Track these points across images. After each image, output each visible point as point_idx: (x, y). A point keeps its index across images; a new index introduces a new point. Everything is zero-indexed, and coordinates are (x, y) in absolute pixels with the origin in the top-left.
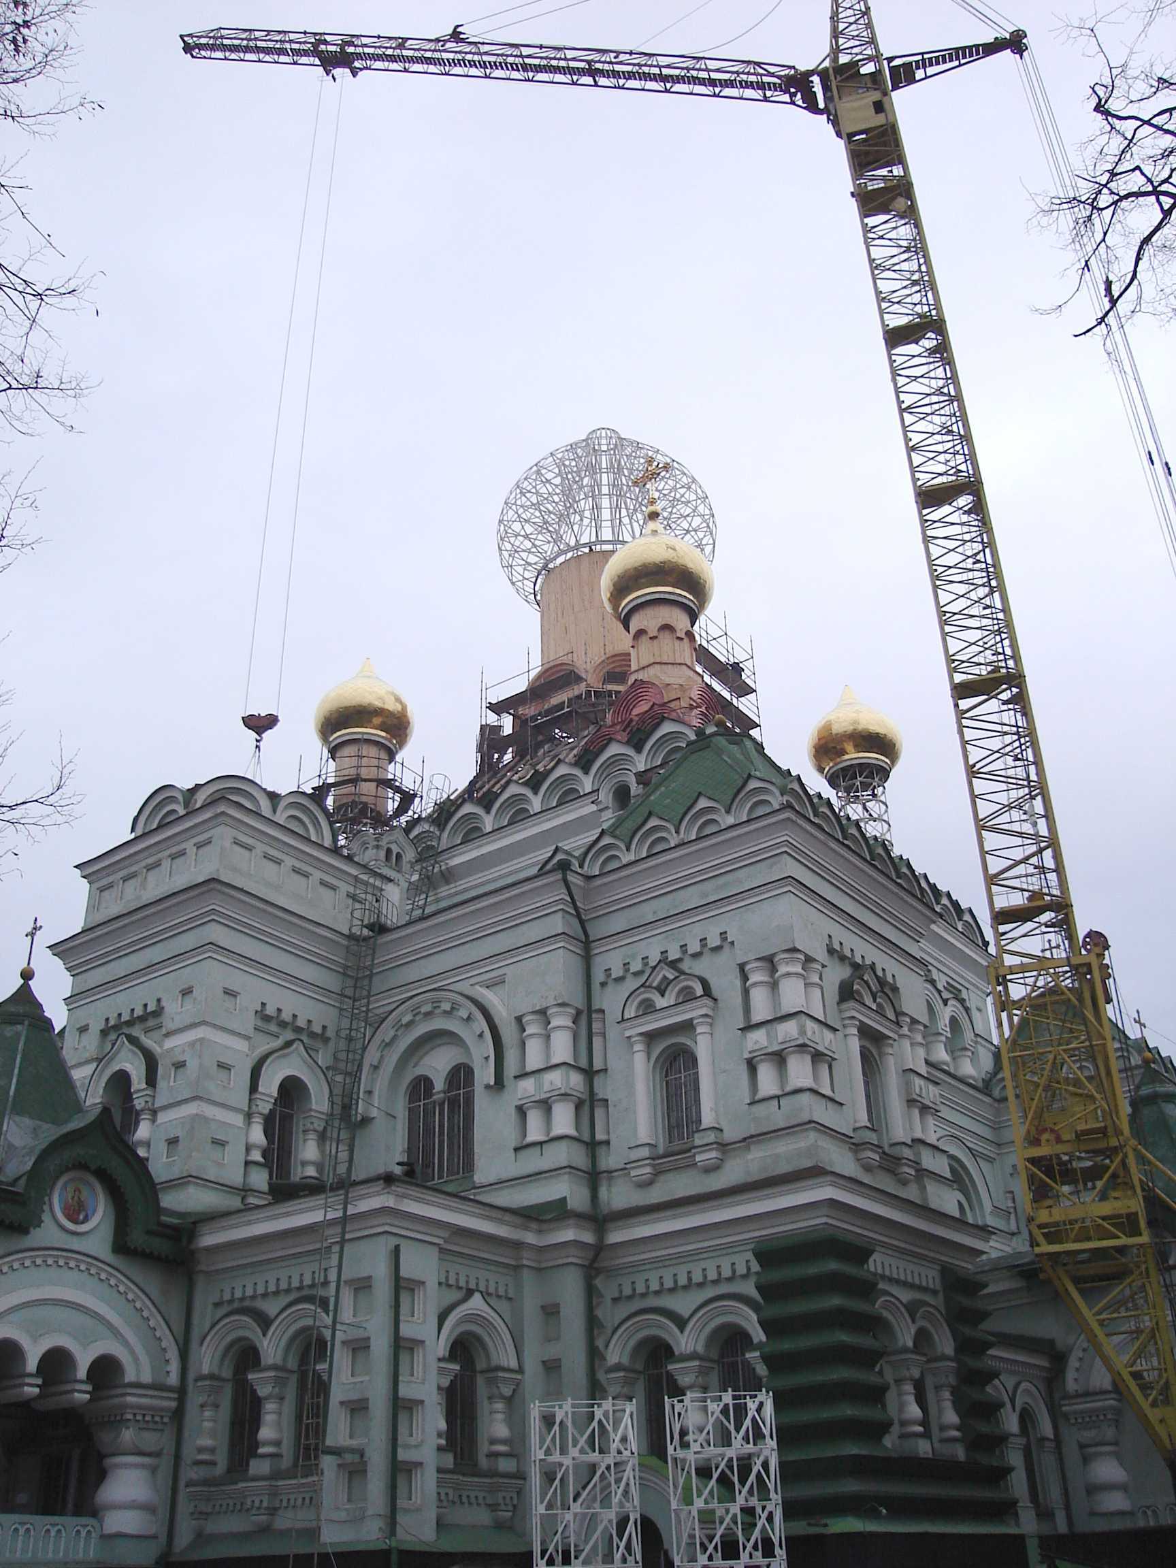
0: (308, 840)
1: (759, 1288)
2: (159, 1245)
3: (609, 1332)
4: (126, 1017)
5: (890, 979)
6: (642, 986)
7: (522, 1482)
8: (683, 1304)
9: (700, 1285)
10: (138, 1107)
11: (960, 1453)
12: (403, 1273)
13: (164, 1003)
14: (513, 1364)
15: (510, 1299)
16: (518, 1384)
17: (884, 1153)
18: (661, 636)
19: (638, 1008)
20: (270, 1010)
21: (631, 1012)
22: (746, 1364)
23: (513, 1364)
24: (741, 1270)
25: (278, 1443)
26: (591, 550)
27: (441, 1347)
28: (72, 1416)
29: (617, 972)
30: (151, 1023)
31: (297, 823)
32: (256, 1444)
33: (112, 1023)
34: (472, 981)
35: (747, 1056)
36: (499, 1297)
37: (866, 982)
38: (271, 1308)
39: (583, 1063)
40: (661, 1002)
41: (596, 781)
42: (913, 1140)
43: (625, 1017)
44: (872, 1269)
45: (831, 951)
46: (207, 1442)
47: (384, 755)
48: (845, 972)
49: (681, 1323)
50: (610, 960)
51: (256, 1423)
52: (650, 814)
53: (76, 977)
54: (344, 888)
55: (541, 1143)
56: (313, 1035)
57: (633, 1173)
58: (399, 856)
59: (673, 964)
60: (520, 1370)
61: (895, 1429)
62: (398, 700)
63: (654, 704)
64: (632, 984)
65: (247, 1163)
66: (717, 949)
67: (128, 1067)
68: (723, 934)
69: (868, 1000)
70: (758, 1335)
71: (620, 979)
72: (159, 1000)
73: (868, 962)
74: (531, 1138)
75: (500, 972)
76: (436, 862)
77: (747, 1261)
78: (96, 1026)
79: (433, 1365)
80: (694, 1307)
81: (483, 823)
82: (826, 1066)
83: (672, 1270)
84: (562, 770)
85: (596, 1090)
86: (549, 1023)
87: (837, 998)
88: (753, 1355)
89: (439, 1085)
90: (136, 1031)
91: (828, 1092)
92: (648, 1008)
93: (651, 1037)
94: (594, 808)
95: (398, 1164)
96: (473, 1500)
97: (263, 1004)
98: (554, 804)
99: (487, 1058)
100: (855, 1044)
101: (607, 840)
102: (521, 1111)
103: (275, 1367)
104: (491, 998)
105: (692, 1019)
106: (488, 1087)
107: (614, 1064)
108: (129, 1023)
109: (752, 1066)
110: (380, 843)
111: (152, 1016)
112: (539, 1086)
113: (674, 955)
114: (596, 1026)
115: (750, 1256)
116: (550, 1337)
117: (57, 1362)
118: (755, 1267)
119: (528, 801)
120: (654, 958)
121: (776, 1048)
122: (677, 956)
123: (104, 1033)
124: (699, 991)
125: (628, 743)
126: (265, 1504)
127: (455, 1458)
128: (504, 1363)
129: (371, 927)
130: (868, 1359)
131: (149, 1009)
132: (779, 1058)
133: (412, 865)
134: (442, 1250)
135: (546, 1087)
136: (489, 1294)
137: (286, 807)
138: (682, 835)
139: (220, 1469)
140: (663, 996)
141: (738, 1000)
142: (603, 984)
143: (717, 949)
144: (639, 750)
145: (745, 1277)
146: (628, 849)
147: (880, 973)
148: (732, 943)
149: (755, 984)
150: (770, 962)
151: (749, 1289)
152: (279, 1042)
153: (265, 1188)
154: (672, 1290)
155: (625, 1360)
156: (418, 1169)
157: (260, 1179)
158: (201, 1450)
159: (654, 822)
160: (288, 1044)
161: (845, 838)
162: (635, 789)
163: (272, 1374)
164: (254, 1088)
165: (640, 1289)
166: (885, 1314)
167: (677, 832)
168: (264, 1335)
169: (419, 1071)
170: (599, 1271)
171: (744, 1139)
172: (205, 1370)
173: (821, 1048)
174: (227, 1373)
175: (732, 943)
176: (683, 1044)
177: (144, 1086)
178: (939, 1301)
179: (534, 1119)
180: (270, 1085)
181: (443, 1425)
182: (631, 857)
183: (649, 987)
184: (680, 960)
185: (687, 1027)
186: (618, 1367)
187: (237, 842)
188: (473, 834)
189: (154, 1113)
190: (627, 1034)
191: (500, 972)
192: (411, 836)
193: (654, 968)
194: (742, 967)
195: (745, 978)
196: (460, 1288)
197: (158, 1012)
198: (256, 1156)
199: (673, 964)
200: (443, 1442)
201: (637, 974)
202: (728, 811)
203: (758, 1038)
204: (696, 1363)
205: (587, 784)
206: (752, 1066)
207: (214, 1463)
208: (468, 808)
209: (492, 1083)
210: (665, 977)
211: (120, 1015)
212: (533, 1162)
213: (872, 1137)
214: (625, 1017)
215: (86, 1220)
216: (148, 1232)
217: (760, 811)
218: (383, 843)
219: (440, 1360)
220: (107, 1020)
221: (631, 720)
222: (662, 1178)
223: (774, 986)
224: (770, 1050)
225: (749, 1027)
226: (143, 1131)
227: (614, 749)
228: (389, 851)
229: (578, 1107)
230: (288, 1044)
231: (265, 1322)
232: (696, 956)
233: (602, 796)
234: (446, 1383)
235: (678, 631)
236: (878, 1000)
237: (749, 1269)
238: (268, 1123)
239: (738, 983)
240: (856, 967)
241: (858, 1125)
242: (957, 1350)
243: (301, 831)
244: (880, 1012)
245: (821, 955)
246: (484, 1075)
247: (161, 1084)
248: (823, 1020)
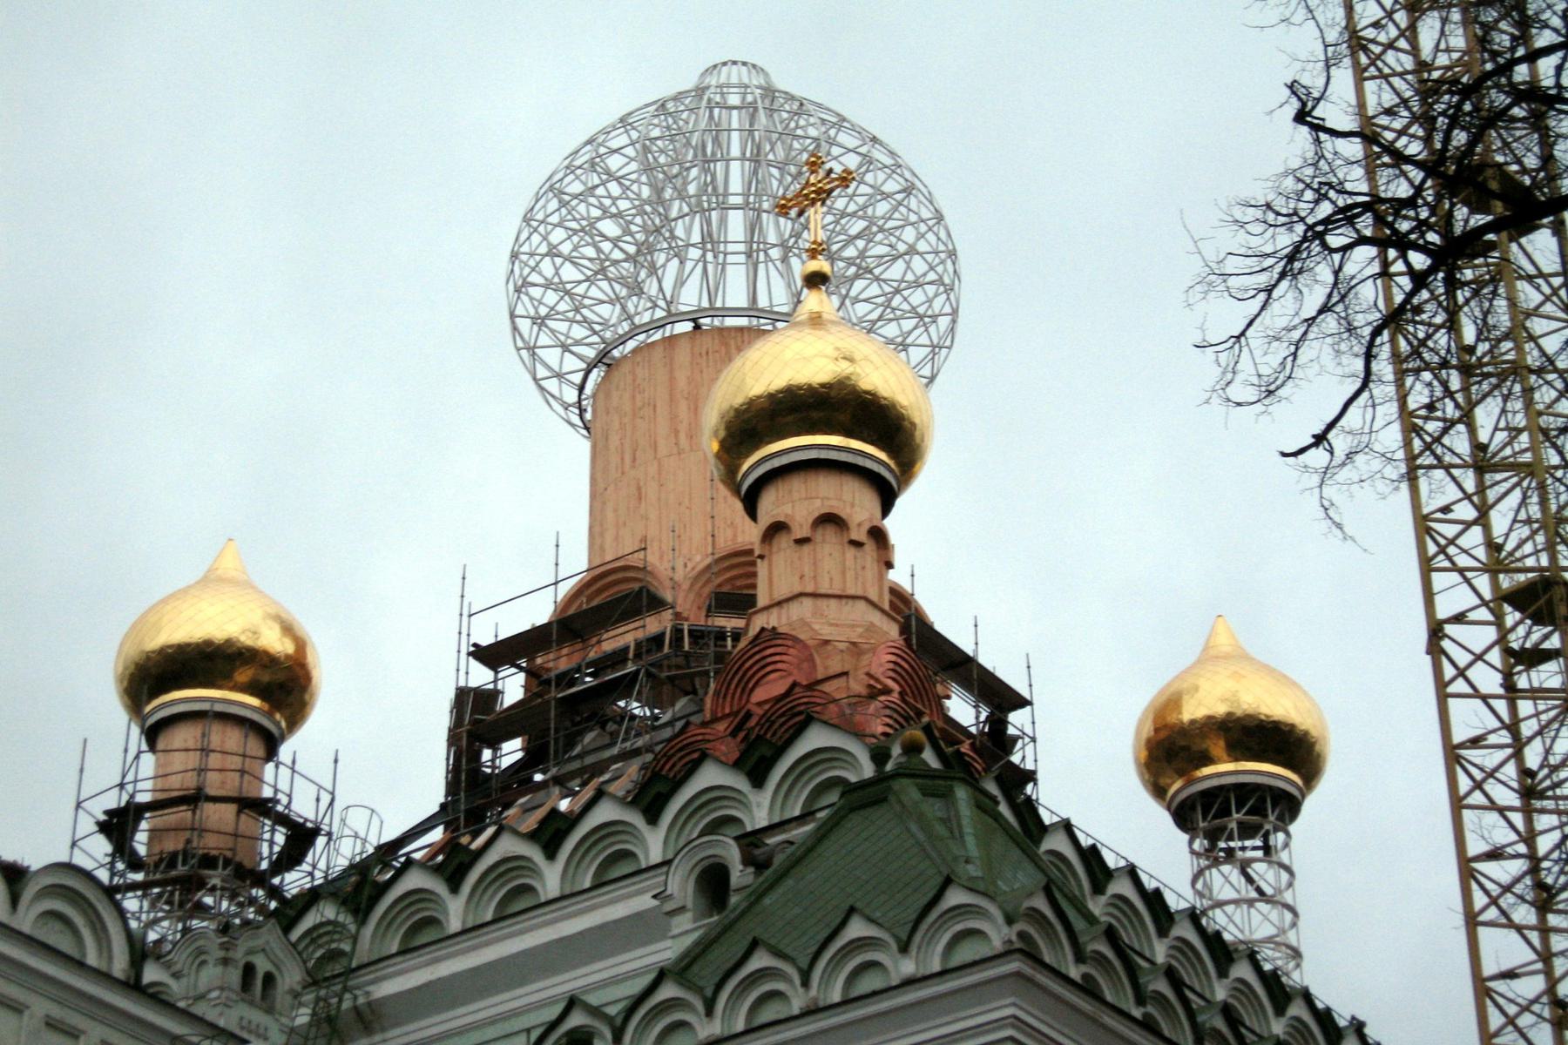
0: (79, 965)
18: (818, 536)
26: (697, 327)
31: (58, 926)
41: (673, 835)
47: (255, 747)
52: (754, 945)
58: (269, 979)
62: (288, 629)
63: (794, 685)
76: (345, 989)
81: (446, 912)
84: (605, 812)
98: (587, 884)
101: (668, 991)
110: (231, 954)
119: (534, 871)
125: (737, 765)
133: (296, 995)
138: (813, 992)
144: (758, 779)
146: (709, 1012)
159: (759, 961)
161: (1140, 1000)
162: (739, 875)
167: (806, 983)
192: (295, 935)
202: (904, 948)
217: (966, 953)
218: (239, 954)
221: (749, 715)
227: (710, 776)
228: (249, 970)
235: (853, 525)
243: (64, 943)
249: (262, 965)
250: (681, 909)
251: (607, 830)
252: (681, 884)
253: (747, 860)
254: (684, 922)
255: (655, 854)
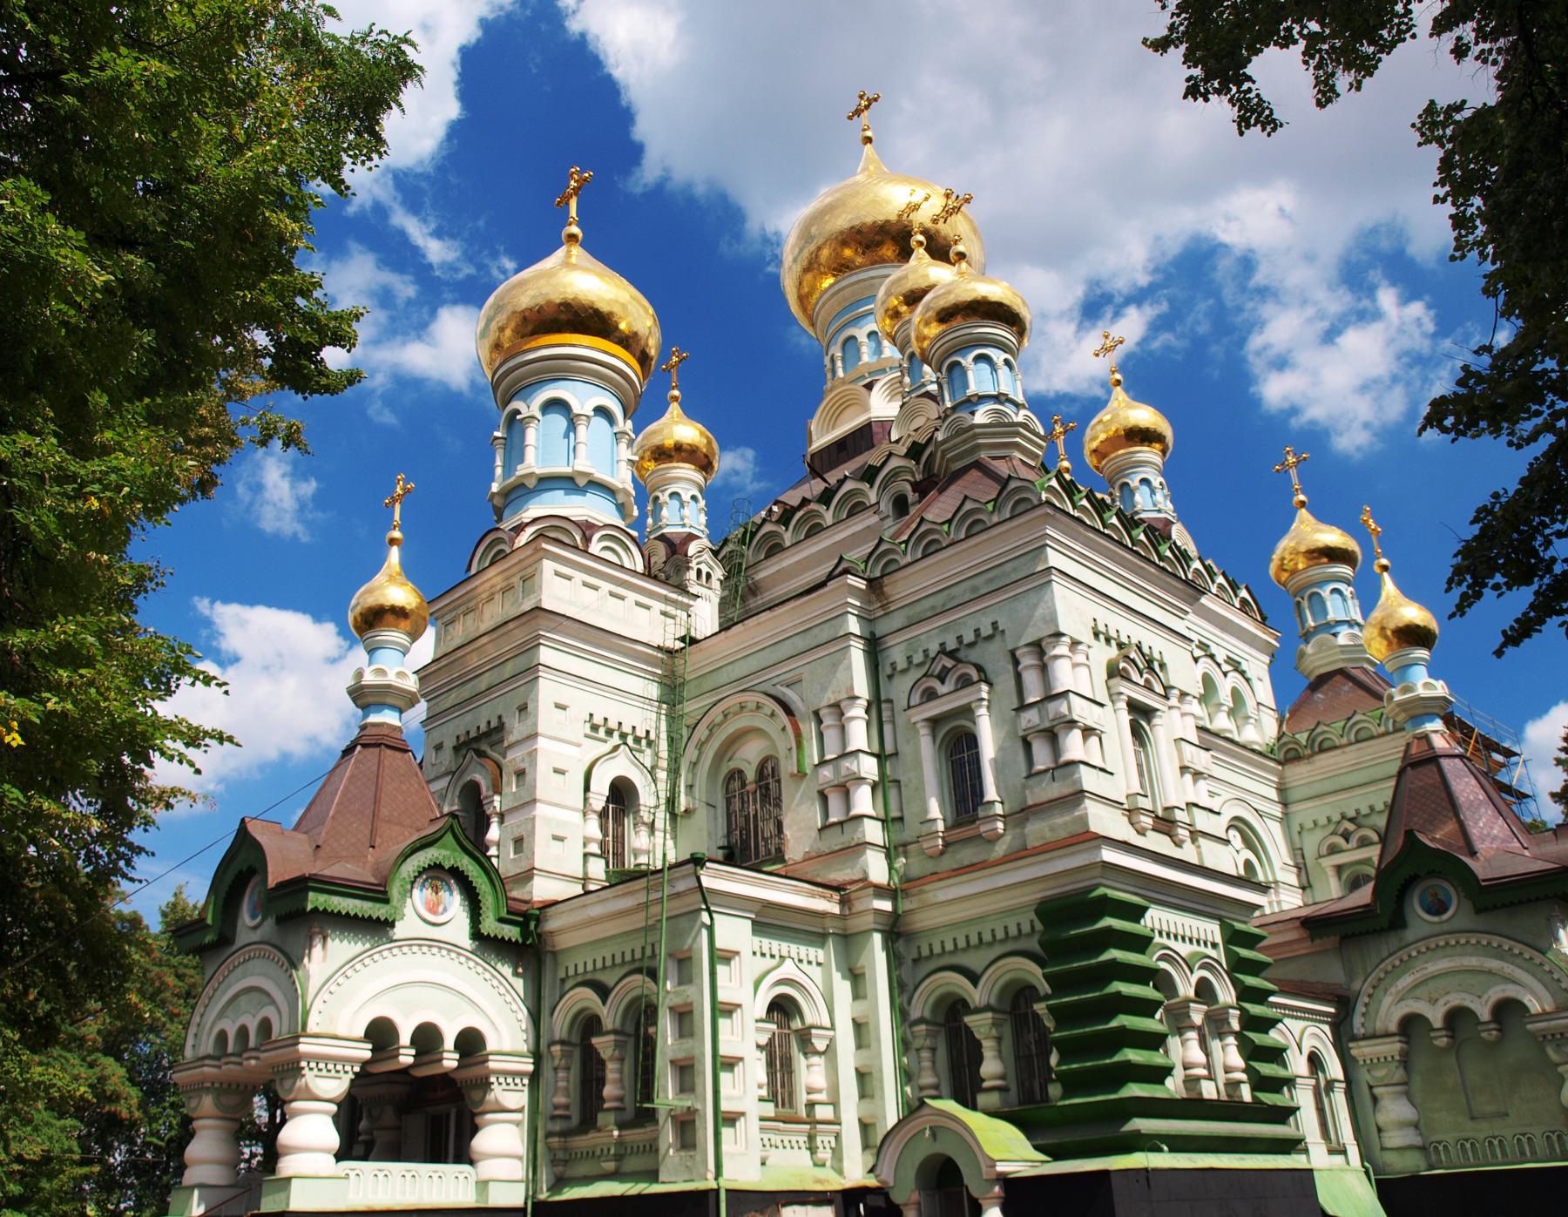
1: (1041, 944)
2: (512, 932)
3: (911, 987)
4: (473, 734)
5: (1157, 656)
6: (925, 675)
7: (837, 1127)
8: (974, 961)
9: (990, 944)
10: (488, 812)
11: (1246, 1094)
12: (718, 944)
13: (504, 720)
14: (827, 1023)
15: (819, 964)
16: (832, 1040)
17: (1157, 817)
19: (922, 695)
20: (598, 720)
21: (916, 699)
22: (1036, 1016)
23: (827, 1023)
24: (1026, 928)
25: (621, 1099)
27: (761, 1011)
28: (446, 1079)
29: (902, 665)
30: (495, 738)
32: (602, 1100)
33: (462, 739)
34: (774, 681)
35: (1021, 733)
36: (810, 963)
37: (1133, 661)
38: (608, 978)
39: (876, 749)
40: (942, 689)
42: (1187, 804)
43: (912, 703)
44: (1149, 924)
45: (1096, 635)
46: (561, 1100)
48: (1113, 652)
49: (974, 978)
50: (896, 654)
51: (602, 1082)
53: (432, 703)
54: (658, 606)
55: (841, 823)
56: (637, 740)
57: (925, 845)
58: (709, 576)
59: (952, 654)
60: (833, 1028)
61: (1179, 1073)
64: (915, 674)
65: (586, 855)
66: (990, 638)
67: (478, 777)
68: (995, 625)
69: (1135, 676)
70: (1045, 987)
71: (904, 671)
72: (500, 717)
73: (1134, 641)
74: (832, 819)
75: (797, 672)
77: (1032, 921)
78: (450, 743)
79: (752, 1025)
80: (987, 963)
81: (783, 539)
82: (1097, 739)
83: (965, 931)
85: (888, 771)
86: (843, 714)
87: (1105, 677)
88: (1040, 1008)
89: (751, 775)
90: (485, 747)
91: (1098, 762)
92: (930, 695)
93: (934, 722)
94: (876, 518)
95: (720, 848)
96: (794, 1144)
97: (591, 715)
99: (790, 749)
100: (1125, 718)
102: (823, 797)
103: (615, 1032)
104: (791, 695)
105: (970, 704)
106: (792, 775)
107: (904, 748)
108: (477, 739)
109: (1027, 745)
111: (495, 733)
112: (837, 771)
113: (951, 645)
114: (886, 715)
115: (1033, 916)
116: (857, 995)
117: (427, 1037)
118: (1039, 926)
119: (821, 516)
120: (934, 648)
121: (1047, 725)
122: (953, 647)
123: (456, 749)
124: (974, 675)
126: (612, 1151)
127: (777, 1106)
128: (817, 1022)
129: (683, 639)
130: (1145, 1008)
131: (493, 725)
132: (1052, 736)
134: (754, 922)
135: (844, 772)
136: (800, 961)
137: (600, 540)
139: (575, 1121)
140: (943, 682)
141: (1012, 683)
142: (890, 677)
143: (990, 638)
145: (1028, 935)
147: (1146, 650)
148: (1003, 632)
149: (1026, 667)
150: (1038, 647)
151: (1033, 945)
152: (608, 747)
153: (603, 877)
154: (964, 950)
155: (927, 1014)
156: (737, 852)
157: (597, 869)
158: (556, 1107)
160: (616, 748)
161: (1104, 527)
162: (912, 497)
163: (612, 1037)
164: (587, 788)
165: (937, 949)
166: (1163, 965)
168: (604, 1003)
169: (733, 765)
170: (899, 935)
171: (1023, 810)
172: (557, 1037)
173: (1090, 723)
174: (576, 1039)
175: (1003, 632)
176: (963, 726)
177: (491, 793)
178: (1219, 954)
179: (835, 802)
180: (601, 787)
181: (763, 1078)
182: (909, 559)
183: (932, 676)
184: (957, 650)
185: (967, 711)
186: (921, 1021)
187: (557, 574)
188: (775, 548)
189: (502, 816)
190: (913, 720)
191: (797, 672)
192: (720, 557)
193: (934, 659)
194: (1013, 653)
195: (1016, 662)
196: (773, 956)
197: (501, 727)
198: (595, 848)
199: (952, 654)
200: (764, 1092)
201: (920, 665)
203: (1031, 718)
204: (990, 1015)
205: (872, 496)
206: (1027, 745)
207: (568, 1118)
208: (768, 528)
209: (795, 771)
210: (944, 667)
211: (468, 733)
212: (835, 840)
213: (1145, 803)
214: (912, 703)
215: (445, 910)
216: (501, 920)
219: (757, 1021)
220: (458, 737)
222: (950, 849)
223: (1044, 669)
224: (1042, 727)
225: (1022, 707)
226: (494, 833)
228: (699, 572)
229: (874, 787)
230: (616, 748)
231: (603, 991)
232: (971, 645)
233: (882, 506)
234: (764, 1040)
236: (1145, 676)
237: (1033, 927)
238: (603, 815)
239: (1010, 667)
240: (1120, 646)
241: (1130, 792)
242: (1238, 999)
243: (614, 559)
244: (1148, 687)
245: (1086, 636)
246: (788, 767)
247: (506, 790)
248: (1091, 697)
249: (705, 569)
250: (888, 516)
251: (850, 493)
252: (886, 507)
253: (914, 491)
254: (889, 522)
255: (873, 500)
